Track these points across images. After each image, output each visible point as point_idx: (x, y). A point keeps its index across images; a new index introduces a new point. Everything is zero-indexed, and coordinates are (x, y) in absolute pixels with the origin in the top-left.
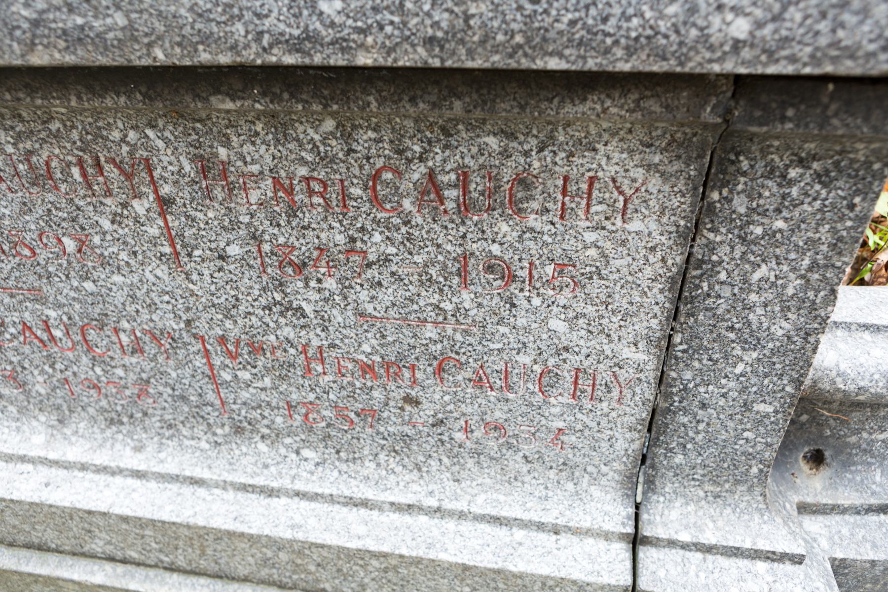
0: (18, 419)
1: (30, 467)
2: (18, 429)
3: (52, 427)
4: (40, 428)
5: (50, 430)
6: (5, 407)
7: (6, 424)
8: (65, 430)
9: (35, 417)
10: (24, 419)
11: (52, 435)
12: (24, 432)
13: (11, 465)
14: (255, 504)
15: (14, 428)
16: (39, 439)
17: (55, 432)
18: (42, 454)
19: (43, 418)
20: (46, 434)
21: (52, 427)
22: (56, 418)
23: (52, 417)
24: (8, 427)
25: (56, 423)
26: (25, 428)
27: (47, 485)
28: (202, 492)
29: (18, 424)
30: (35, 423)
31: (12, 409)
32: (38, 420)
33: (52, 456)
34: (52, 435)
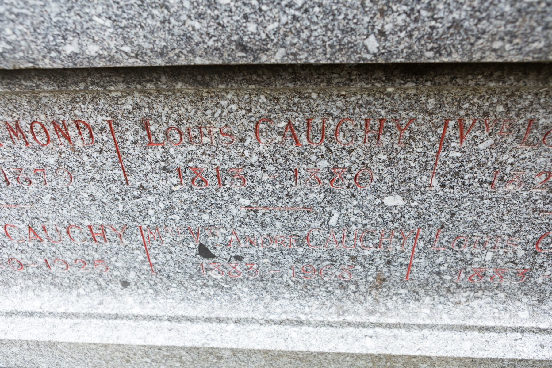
0: (504, 302)
1: (519, 335)
2: (505, 309)
3: (533, 305)
4: (523, 307)
5: (531, 308)
6: (496, 294)
7: (495, 306)
8: (543, 307)
9: (519, 300)
10: (510, 302)
11: (534, 311)
12: (510, 310)
13: (503, 335)
15: (502, 308)
16: (525, 314)
17: (535, 309)
18: (534, 325)
19: (525, 300)
20: (529, 311)
21: (533, 305)
22: (536, 299)
23: (533, 299)
24: (497, 308)
25: (536, 302)
26: (511, 307)
27: (542, 346)
29: (505, 305)
30: (518, 304)
31: (502, 295)
32: (521, 302)
33: (542, 326)
34: (534, 311)
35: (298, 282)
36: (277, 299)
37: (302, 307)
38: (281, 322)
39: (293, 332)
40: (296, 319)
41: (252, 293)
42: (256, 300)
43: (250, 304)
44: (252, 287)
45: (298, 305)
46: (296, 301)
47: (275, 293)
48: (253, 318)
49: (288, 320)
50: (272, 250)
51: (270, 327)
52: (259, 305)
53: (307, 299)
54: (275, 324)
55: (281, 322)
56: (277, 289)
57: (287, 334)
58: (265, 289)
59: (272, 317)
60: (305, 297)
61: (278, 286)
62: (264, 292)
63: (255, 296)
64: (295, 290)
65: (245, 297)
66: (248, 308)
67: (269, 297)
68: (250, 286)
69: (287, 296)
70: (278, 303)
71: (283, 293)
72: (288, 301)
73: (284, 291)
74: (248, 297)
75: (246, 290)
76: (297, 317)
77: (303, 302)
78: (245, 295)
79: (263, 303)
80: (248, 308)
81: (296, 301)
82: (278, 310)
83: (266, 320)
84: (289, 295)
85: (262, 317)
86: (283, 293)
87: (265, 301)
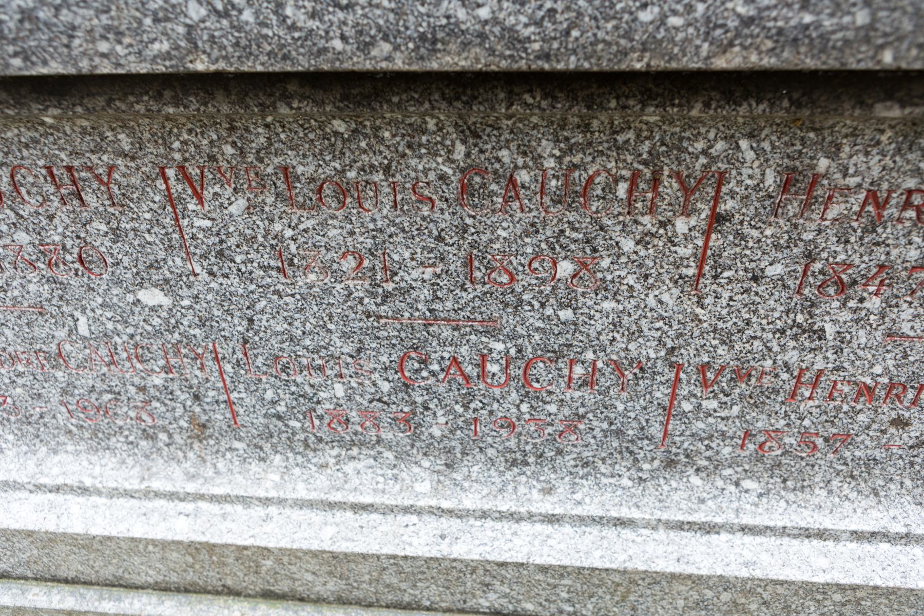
0: (395, 466)
1: (414, 518)
2: (395, 478)
3: (438, 472)
4: (423, 474)
5: (435, 477)
6: (380, 453)
7: (379, 472)
8: (455, 475)
9: (416, 463)
10: (403, 466)
11: (439, 481)
12: (403, 480)
13: (390, 518)
14: (695, 545)
15: (390, 476)
16: (424, 487)
17: (442, 478)
18: (433, 502)
19: (426, 463)
20: (431, 481)
21: (438, 472)
22: (443, 462)
23: (438, 462)
24: (383, 475)
25: (443, 468)
26: (404, 475)
27: (443, 537)
28: (627, 533)
29: (395, 471)
30: (416, 469)
31: (389, 455)
32: (420, 466)
33: (445, 505)
34: (439, 481)
35: (82, 426)
36: (55, 452)
37: (91, 466)
38: (57, 489)
39: (75, 502)
40: (77, 484)
41: (19, 443)
42: (26, 453)
43: (16, 460)
44: (19, 433)
45: (85, 463)
46: (83, 456)
47: (52, 443)
48: (15, 482)
49: (66, 485)
50: (20, 375)
51: (44, 496)
52: (29, 462)
53: (100, 454)
54: (50, 491)
55: (57, 489)
56: (54, 437)
57: (64, 507)
58: (38, 436)
59: (44, 480)
60: (97, 450)
61: (56, 432)
62: (37, 441)
63: (25, 448)
64: (82, 439)
65: (9, 449)
66: (12, 466)
67: (44, 449)
68: (16, 432)
69: (70, 448)
70: (57, 458)
71: (64, 444)
72: (71, 456)
73: (66, 441)
74: (14, 449)
75: (11, 437)
76: (81, 482)
77: (94, 458)
78: (10, 446)
79: (35, 458)
80: (12, 466)
81: (83, 456)
82: (56, 471)
83: (34, 485)
84: (73, 447)
85: (28, 480)
86: (64, 444)
87: (38, 456)
